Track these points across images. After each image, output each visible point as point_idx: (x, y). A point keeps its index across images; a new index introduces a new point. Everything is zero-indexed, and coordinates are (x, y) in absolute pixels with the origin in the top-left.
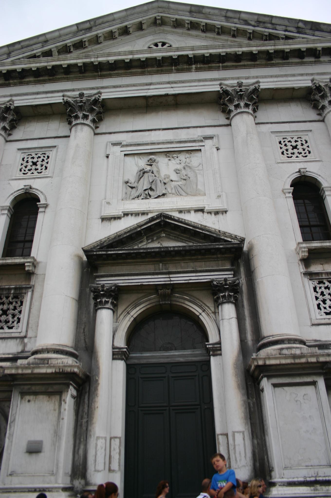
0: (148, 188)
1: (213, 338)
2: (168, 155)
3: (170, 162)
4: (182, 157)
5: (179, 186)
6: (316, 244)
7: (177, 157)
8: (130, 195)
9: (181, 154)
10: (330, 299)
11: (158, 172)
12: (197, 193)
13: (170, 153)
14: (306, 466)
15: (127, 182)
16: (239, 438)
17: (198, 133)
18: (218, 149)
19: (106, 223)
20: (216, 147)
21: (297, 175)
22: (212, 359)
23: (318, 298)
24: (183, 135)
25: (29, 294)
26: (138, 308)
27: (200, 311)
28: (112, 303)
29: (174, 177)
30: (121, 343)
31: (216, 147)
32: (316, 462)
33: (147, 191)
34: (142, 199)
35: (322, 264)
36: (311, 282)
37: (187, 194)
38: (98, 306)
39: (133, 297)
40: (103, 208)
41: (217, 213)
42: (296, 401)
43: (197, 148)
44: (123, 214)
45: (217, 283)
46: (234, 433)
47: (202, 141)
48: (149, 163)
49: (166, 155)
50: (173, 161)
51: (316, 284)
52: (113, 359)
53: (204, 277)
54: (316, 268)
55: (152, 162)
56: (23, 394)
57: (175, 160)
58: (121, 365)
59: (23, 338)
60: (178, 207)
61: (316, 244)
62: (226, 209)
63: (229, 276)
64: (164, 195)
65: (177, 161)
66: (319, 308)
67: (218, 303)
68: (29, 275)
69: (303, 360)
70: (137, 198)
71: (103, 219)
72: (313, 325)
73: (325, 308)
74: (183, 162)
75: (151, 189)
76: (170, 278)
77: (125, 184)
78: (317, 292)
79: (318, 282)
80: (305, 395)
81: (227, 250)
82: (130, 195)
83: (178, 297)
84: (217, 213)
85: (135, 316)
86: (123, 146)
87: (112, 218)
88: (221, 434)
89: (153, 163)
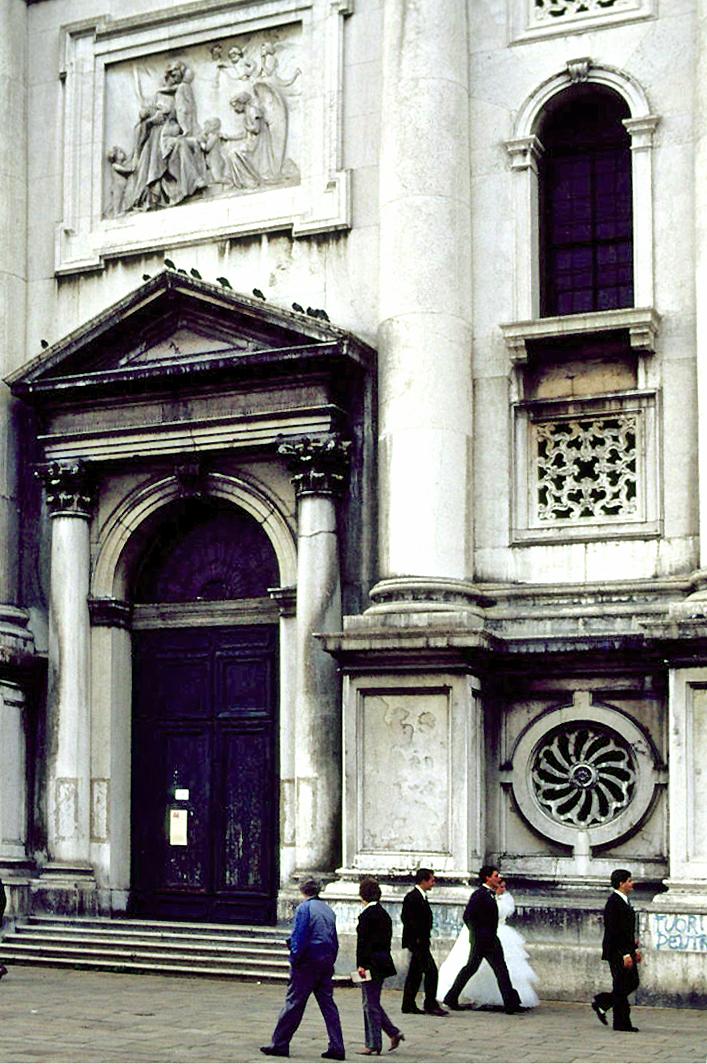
0: (160, 176)
2: (216, 49)
3: (222, 74)
5: (238, 157)
7: (241, 55)
8: (122, 198)
9: (250, 43)
10: (576, 474)
11: (192, 112)
12: (286, 176)
13: (220, 43)
14: (402, 851)
15: (113, 160)
18: (347, 16)
20: (341, 12)
21: (560, 84)
23: (546, 473)
26: (138, 509)
27: (265, 512)
28: (81, 503)
29: (231, 125)
30: (109, 589)
31: (341, 12)
32: (422, 845)
33: (157, 185)
34: (149, 210)
35: (572, 378)
36: (535, 429)
37: (259, 183)
39: (130, 483)
40: (57, 248)
42: (404, 726)
43: (292, 18)
44: (103, 262)
45: (288, 449)
46: (298, 778)
48: (165, 89)
49: (212, 51)
51: (548, 435)
52: (93, 624)
53: (264, 433)
54: (553, 388)
55: (176, 83)
57: (237, 65)
60: (228, 231)
62: (346, 225)
64: (199, 192)
65: (240, 69)
66: (543, 500)
69: (420, 643)
70: (136, 209)
72: (513, 546)
73: (558, 499)
74: (255, 69)
75: (168, 177)
76: (192, 437)
77: (108, 164)
78: (546, 457)
79: (553, 429)
80: (424, 714)
82: (122, 198)
83: (219, 480)
85: (133, 527)
86: (101, 37)
87: (80, 274)
88: (289, 781)
89: (175, 86)
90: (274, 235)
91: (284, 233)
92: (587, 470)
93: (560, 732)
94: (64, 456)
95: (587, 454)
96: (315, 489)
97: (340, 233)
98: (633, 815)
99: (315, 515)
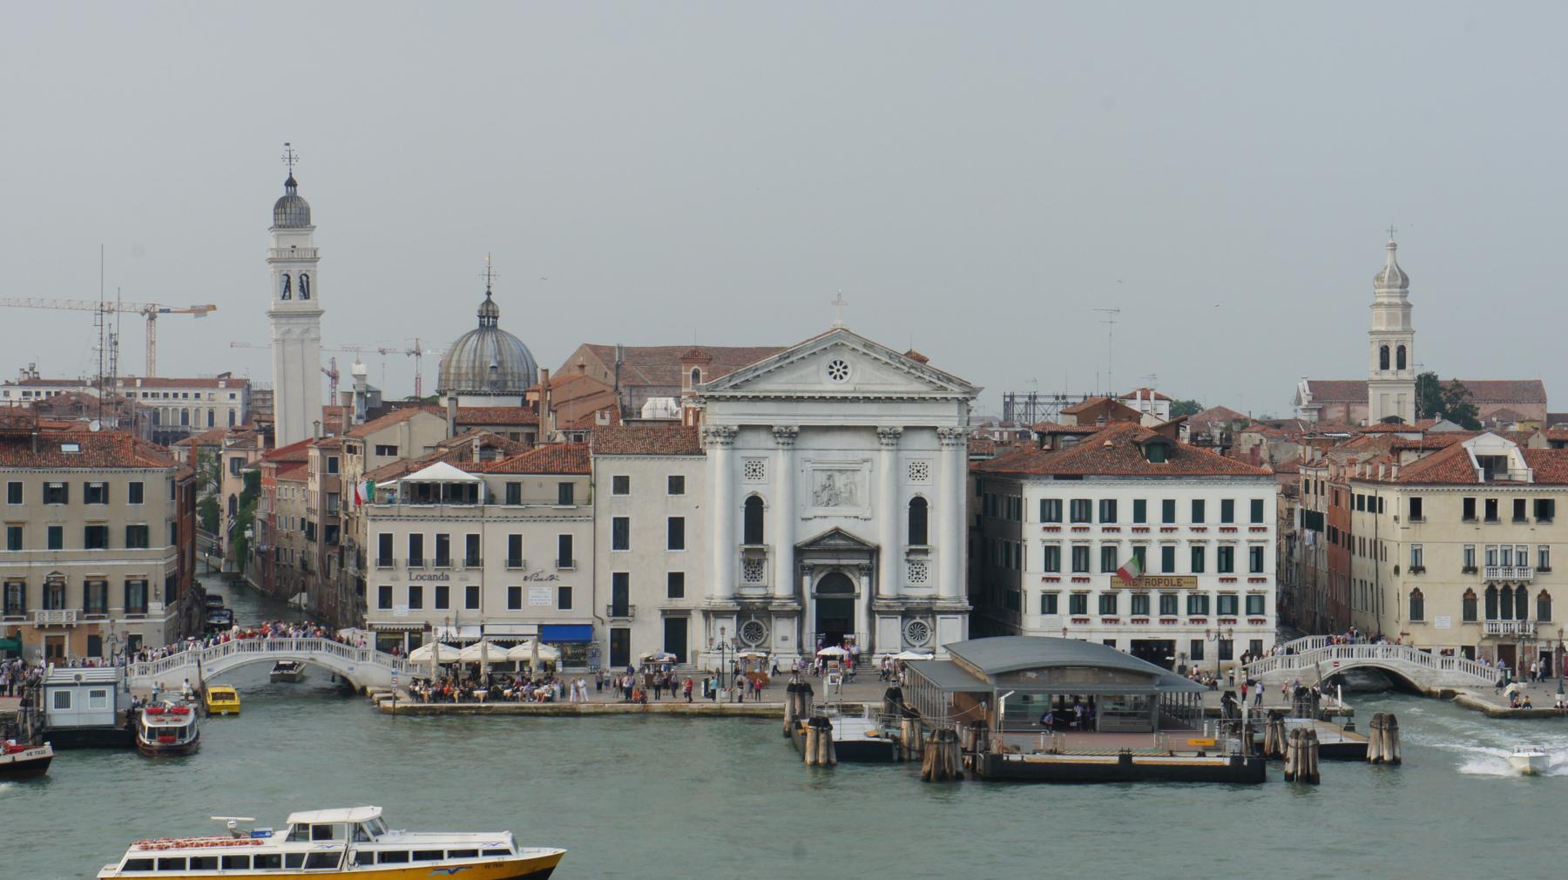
1: (857, 591)
4: (849, 473)
6: (914, 547)
12: (855, 505)
16: (864, 636)
17: (860, 455)
19: (804, 522)
21: (915, 496)
22: (856, 601)
24: (851, 456)
30: (814, 591)
38: (803, 575)
41: (865, 520)
53: (856, 562)
54: (912, 557)
58: (814, 601)
59: (766, 587)
61: (914, 547)
67: (861, 574)
71: (803, 519)
81: (868, 550)
84: (865, 520)
90: (855, 517)
91: (857, 517)
94: (808, 562)
95: (918, 570)
96: (866, 575)
97: (870, 519)
98: (926, 640)
99: (865, 580)
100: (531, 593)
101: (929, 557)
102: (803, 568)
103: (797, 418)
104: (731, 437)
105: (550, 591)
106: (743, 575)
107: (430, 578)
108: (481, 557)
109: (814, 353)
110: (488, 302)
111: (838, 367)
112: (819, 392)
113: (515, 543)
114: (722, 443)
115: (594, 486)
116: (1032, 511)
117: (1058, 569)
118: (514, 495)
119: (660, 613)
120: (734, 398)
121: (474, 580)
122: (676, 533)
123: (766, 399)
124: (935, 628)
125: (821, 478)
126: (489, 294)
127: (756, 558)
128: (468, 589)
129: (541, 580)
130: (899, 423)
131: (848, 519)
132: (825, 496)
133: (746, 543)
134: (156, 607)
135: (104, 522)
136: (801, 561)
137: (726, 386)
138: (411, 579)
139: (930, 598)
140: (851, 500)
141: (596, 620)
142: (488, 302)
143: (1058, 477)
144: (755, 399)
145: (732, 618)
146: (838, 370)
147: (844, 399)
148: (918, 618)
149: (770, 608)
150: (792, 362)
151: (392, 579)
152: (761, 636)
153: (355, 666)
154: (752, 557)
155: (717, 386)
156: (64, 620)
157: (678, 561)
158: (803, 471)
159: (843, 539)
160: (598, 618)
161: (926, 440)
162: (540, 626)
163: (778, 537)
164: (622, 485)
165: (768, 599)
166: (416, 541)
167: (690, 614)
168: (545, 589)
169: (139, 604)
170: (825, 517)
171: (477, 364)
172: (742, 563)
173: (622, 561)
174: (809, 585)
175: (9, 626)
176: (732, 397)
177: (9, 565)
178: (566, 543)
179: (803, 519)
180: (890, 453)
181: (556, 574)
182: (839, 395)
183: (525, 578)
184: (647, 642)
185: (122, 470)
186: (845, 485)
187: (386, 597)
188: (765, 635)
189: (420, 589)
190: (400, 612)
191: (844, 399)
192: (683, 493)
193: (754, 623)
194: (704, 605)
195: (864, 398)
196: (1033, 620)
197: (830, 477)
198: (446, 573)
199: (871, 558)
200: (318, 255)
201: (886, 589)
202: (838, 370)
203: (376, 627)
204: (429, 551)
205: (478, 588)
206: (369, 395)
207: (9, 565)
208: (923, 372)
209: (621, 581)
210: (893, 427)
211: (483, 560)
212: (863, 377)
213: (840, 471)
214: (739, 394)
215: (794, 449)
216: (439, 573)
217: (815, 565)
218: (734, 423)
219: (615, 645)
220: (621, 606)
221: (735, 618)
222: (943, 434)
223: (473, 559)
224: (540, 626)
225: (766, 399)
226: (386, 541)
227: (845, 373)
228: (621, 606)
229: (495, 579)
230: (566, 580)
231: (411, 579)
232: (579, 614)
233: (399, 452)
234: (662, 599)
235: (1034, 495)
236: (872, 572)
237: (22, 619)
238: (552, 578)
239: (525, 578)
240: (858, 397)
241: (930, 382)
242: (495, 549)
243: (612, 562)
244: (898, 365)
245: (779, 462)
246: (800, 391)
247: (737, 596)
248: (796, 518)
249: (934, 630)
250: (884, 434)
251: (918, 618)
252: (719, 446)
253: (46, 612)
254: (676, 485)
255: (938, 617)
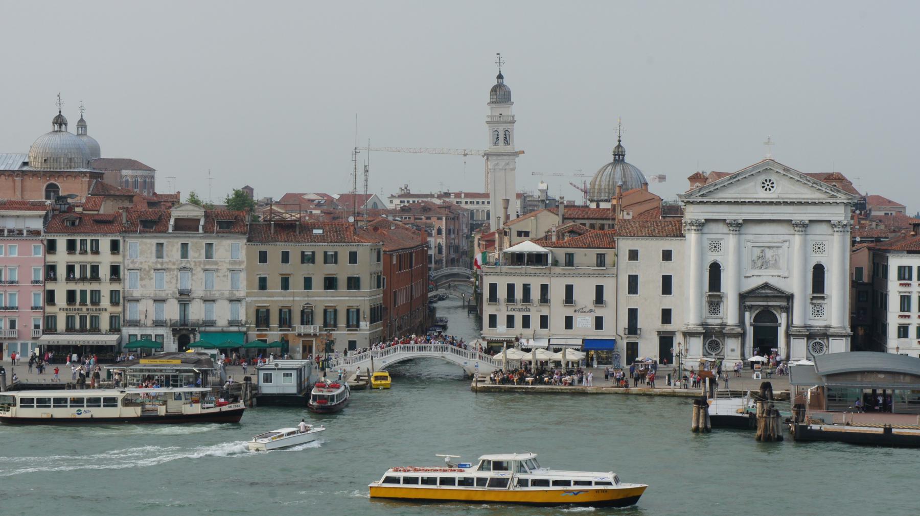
1: (779, 322)
4: (775, 249)
6: (815, 295)
12: (779, 268)
17: (782, 238)
19: (746, 279)
21: (817, 263)
22: (779, 328)
24: (776, 238)
25: (722, 304)
30: (752, 321)
38: (745, 311)
41: (785, 278)
47: (782, 243)
50: (771, 250)
53: (778, 304)
54: (814, 301)
56: (728, 337)
58: (752, 328)
59: (722, 318)
61: (815, 295)
63: (785, 304)
67: (781, 311)
68: (721, 298)
84: (785, 278)
90: (778, 276)
91: (780, 276)
92: (818, 311)
93: (815, 343)
94: (748, 303)
95: (818, 309)
96: (784, 312)
97: (788, 277)
99: (784, 315)
100: (578, 320)
101: (826, 301)
102: (745, 307)
103: (742, 214)
104: (700, 226)
105: (590, 319)
106: (708, 311)
107: (519, 310)
108: (549, 298)
109: (752, 175)
110: (619, 146)
111: (768, 183)
112: (756, 198)
113: (569, 289)
114: (695, 230)
115: (617, 256)
116: (893, 273)
117: (909, 310)
118: (570, 260)
119: (657, 333)
120: (701, 202)
121: (545, 312)
122: (667, 285)
123: (722, 203)
124: (829, 345)
125: (757, 252)
126: (620, 141)
127: (716, 300)
128: (542, 317)
129: (585, 312)
130: (806, 218)
131: (774, 277)
132: (759, 263)
133: (710, 291)
134: (364, 325)
135: (335, 274)
136: (744, 303)
137: (697, 195)
138: (507, 311)
139: (826, 327)
140: (776, 265)
141: (618, 337)
142: (619, 146)
143: (909, 252)
144: (715, 203)
145: (700, 337)
146: (768, 185)
147: (771, 203)
148: (818, 339)
149: (724, 331)
150: (739, 180)
151: (497, 310)
152: (719, 348)
153: (468, 362)
154: (713, 300)
155: (691, 195)
156: (312, 331)
157: (668, 302)
158: (745, 247)
159: (770, 290)
160: (619, 335)
161: (824, 228)
162: (584, 340)
163: (729, 288)
164: (633, 255)
165: (723, 325)
166: (511, 288)
167: (675, 334)
168: (587, 318)
169: (355, 323)
170: (759, 276)
171: (611, 183)
172: (707, 303)
173: (634, 301)
174: (749, 317)
175: (257, 334)
176: (701, 202)
177: (282, 299)
178: (599, 290)
179: (745, 277)
180: (800, 236)
181: (593, 308)
182: (768, 201)
183: (575, 311)
184: (649, 351)
185: (345, 244)
186: (773, 256)
187: (493, 320)
188: (721, 348)
189: (513, 316)
190: (501, 330)
191: (771, 203)
192: (671, 260)
193: (714, 341)
194: (684, 329)
195: (784, 202)
196: (893, 341)
197: (762, 251)
198: (528, 307)
199: (788, 302)
200: (515, 119)
201: (797, 321)
202: (768, 185)
203: (487, 338)
204: (519, 294)
205: (547, 316)
206: (547, 202)
207: (282, 299)
208: (821, 186)
209: (633, 313)
210: (802, 220)
211: (550, 300)
212: (783, 189)
213: (769, 247)
214: (705, 200)
215: (740, 234)
216: (524, 307)
217: (752, 305)
218: (702, 218)
219: (630, 352)
220: (633, 329)
221: (702, 337)
222: (835, 225)
223: (544, 299)
224: (584, 340)
225: (722, 203)
226: (493, 287)
227: (773, 187)
228: (633, 329)
229: (557, 311)
230: (599, 312)
231: (507, 311)
232: (607, 333)
233: (530, 235)
234: (658, 324)
235: (894, 263)
236: (788, 310)
237: (289, 330)
238: (591, 311)
239: (575, 311)
240: (780, 202)
241: (826, 192)
242: (557, 293)
243: (628, 301)
244: (805, 182)
245: (730, 241)
246: (743, 198)
247: (704, 324)
248: (740, 276)
249: (828, 347)
250: (796, 225)
251: (818, 339)
252: (693, 232)
253: (302, 326)
254: (667, 255)
255: (830, 339)
